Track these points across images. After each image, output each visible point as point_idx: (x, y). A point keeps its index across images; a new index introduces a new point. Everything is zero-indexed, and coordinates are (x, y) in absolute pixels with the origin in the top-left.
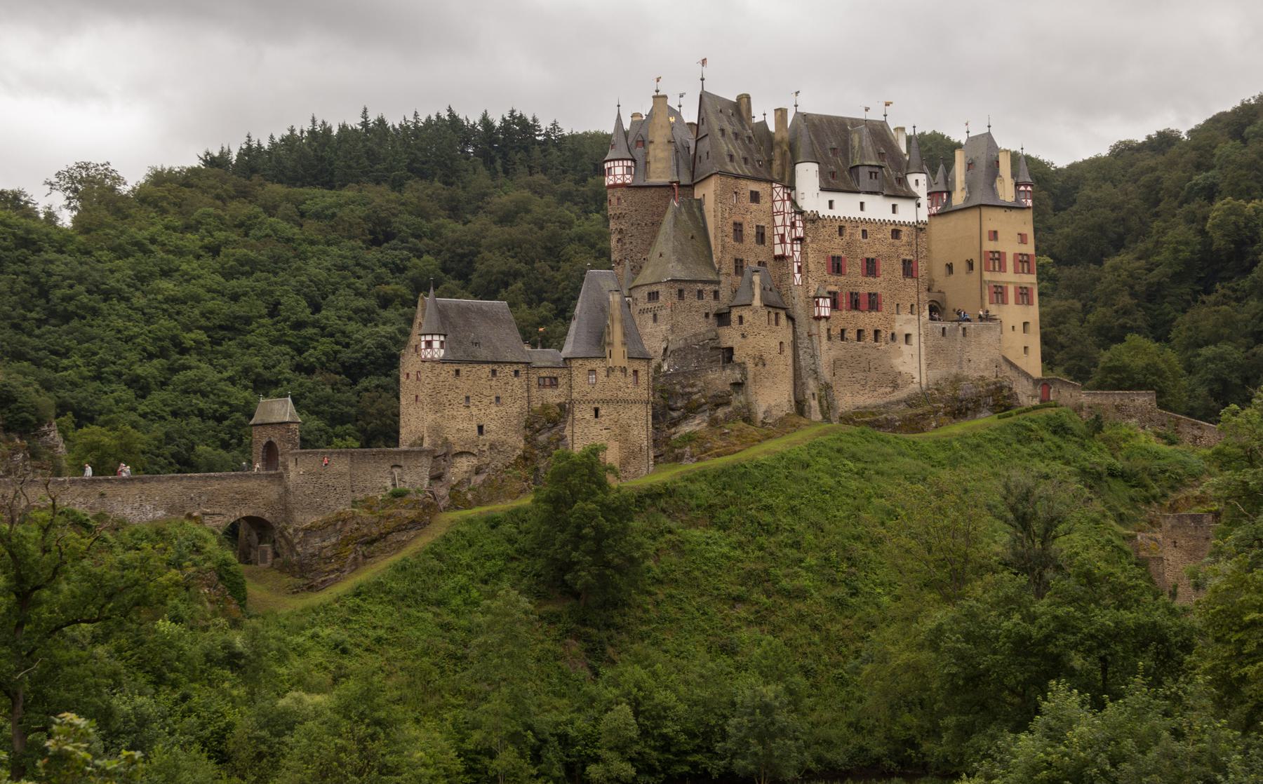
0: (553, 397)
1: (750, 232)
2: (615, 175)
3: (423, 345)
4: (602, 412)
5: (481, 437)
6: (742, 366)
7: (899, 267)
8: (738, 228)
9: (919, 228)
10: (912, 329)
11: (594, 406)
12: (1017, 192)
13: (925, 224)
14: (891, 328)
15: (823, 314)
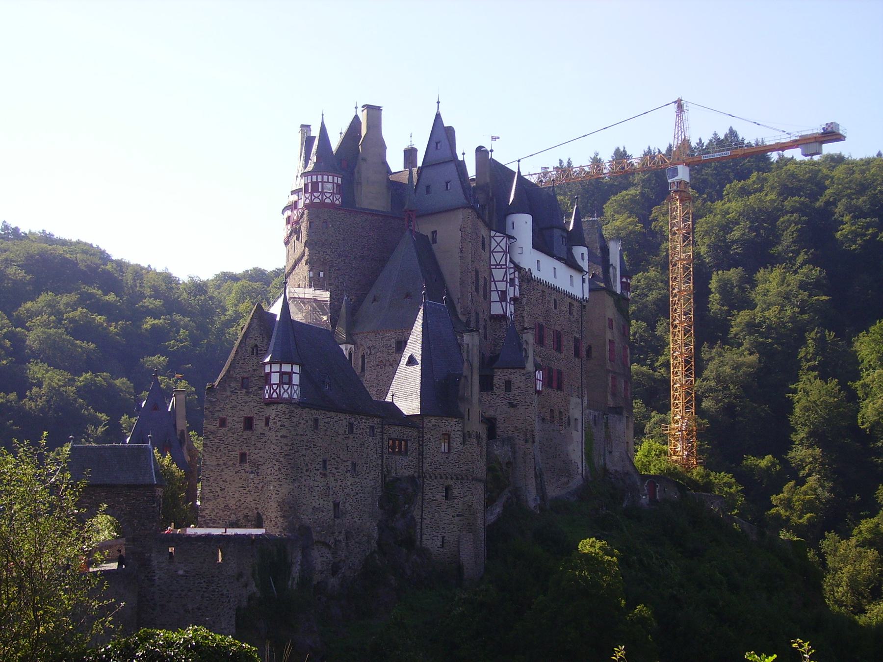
0: (403, 467)
1: (481, 282)
2: (323, 193)
3: (275, 379)
4: (456, 492)
5: (337, 521)
6: (509, 440)
7: (572, 344)
8: (477, 272)
9: (583, 304)
10: (576, 412)
11: (446, 484)
12: (622, 283)
13: (587, 301)
14: (568, 410)
15: (538, 389)
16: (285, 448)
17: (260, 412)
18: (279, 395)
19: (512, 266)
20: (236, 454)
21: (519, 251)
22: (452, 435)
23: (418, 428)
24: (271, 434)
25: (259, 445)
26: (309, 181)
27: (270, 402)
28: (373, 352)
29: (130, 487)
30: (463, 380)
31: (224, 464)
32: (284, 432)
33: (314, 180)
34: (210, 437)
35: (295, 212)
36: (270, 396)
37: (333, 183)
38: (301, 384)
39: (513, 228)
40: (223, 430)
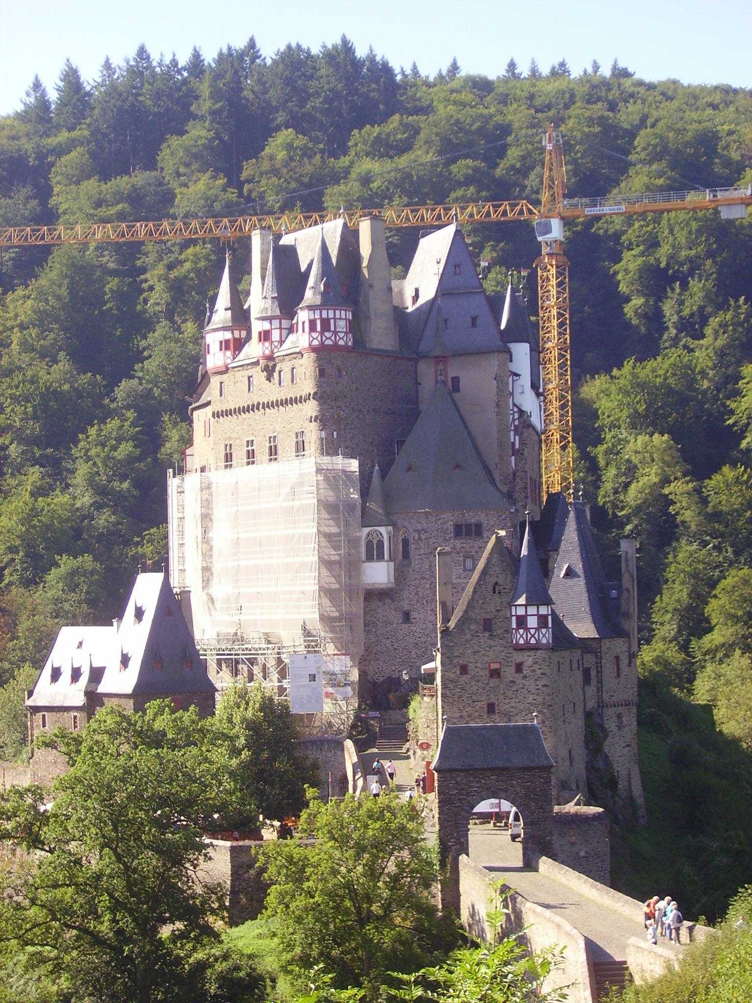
2: (335, 333)
3: (532, 622)
4: (624, 719)
16: (548, 698)
17: (509, 658)
18: (538, 641)
19: (516, 409)
20: (484, 704)
21: (520, 390)
22: (621, 658)
23: (596, 653)
24: (526, 683)
25: (509, 694)
26: (317, 316)
27: (518, 648)
28: (423, 537)
29: (524, 769)
30: (625, 595)
31: (469, 716)
32: (544, 681)
33: (324, 315)
34: (450, 686)
35: (267, 344)
36: (527, 642)
37: (346, 319)
38: (552, 627)
39: (511, 361)
40: (464, 678)
